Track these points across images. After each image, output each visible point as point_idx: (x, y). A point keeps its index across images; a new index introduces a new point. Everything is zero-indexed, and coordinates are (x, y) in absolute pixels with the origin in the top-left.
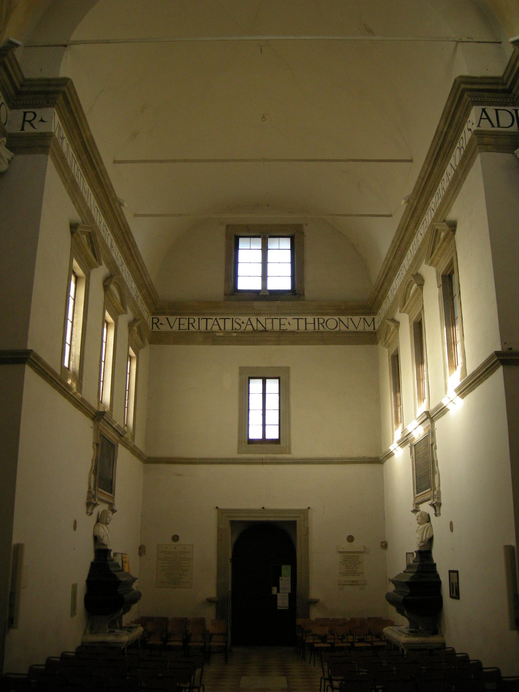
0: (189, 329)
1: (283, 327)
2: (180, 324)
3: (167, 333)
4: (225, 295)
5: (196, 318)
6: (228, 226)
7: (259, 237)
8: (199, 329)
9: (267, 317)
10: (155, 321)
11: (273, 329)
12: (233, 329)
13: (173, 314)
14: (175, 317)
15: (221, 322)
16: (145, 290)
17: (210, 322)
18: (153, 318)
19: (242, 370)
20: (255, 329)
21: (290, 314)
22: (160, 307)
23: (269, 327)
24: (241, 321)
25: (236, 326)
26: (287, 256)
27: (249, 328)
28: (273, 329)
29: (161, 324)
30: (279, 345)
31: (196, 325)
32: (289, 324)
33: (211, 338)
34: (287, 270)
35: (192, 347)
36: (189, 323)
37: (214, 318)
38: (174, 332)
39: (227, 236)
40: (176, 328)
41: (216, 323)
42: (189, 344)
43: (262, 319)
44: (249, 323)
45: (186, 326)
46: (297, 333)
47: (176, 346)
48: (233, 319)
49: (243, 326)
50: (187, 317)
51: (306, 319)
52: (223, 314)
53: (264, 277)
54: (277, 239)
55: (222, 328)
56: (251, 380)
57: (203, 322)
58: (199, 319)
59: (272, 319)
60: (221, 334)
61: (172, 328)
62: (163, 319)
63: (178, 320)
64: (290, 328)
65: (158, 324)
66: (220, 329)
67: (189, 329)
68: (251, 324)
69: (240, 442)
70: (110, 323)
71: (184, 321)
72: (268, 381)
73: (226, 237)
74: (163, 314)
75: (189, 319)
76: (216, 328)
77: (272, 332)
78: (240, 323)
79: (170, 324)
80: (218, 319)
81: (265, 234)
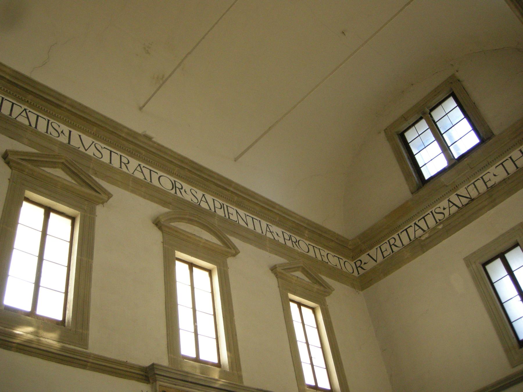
0: (393, 252)
1: (489, 184)
2: (382, 253)
3: (373, 270)
4: (412, 193)
5: (395, 236)
6: (385, 131)
7: (421, 118)
8: (403, 245)
9: (466, 186)
10: (358, 263)
11: (479, 193)
12: (437, 222)
13: (371, 248)
14: (375, 248)
15: (422, 224)
16: (307, 232)
17: (411, 231)
18: (355, 263)
19: (468, 261)
20: (460, 205)
21: (489, 165)
22: (352, 248)
23: (474, 194)
24: (442, 208)
25: (439, 217)
26: (458, 114)
27: (454, 209)
28: (479, 193)
29: (365, 263)
30: (496, 205)
31: (398, 243)
32: (495, 175)
33: (419, 246)
34: (465, 126)
35: (404, 268)
36: (390, 246)
37: (412, 224)
38: (380, 264)
39: (390, 139)
40: (380, 259)
41: (417, 228)
42: (400, 267)
43: (462, 191)
44: (451, 204)
45: (389, 251)
46: (509, 178)
47: (388, 277)
48: (432, 212)
49: (446, 212)
50: (386, 241)
51: (510, 158)
52: (418, 213)
53: (445, 148)
54: (440, 107)
55: (425, 228)
56: (488, 267)
57: (404, 236)
58: (398, 235)
59: (474, 183)
60: (427, 235)
61: (376, 261)
62: (364, 257)
63: (379, 249)
64: (497, 180)
65: (362, 266)
66: (424, 231)
67: (393, 252)
68: (454, 204)
69: (507, 351)
70: (213, 269)
71: (385, 247)
72: (508, 256)
73: (388, 140)
74: (362, 252)
75: (389, 241)
76: (419, 232)
77: (480, 196)
78: (442, 210)
79: (372, 259)
80: (417, 223)
81: (425, 112)
